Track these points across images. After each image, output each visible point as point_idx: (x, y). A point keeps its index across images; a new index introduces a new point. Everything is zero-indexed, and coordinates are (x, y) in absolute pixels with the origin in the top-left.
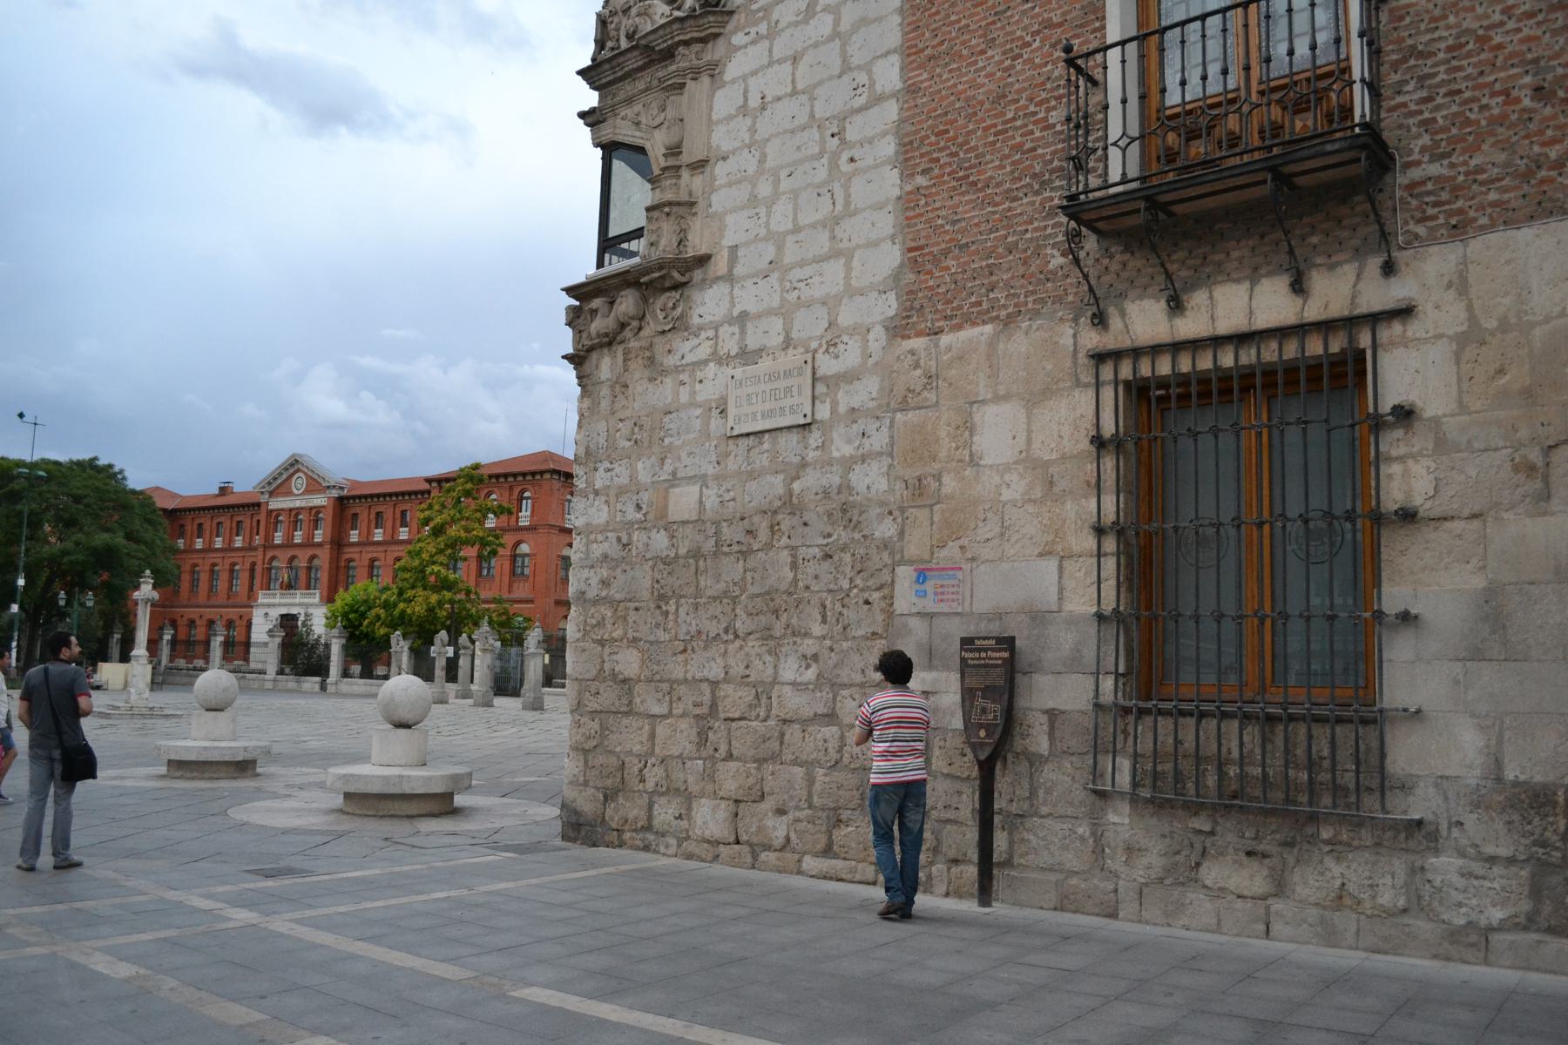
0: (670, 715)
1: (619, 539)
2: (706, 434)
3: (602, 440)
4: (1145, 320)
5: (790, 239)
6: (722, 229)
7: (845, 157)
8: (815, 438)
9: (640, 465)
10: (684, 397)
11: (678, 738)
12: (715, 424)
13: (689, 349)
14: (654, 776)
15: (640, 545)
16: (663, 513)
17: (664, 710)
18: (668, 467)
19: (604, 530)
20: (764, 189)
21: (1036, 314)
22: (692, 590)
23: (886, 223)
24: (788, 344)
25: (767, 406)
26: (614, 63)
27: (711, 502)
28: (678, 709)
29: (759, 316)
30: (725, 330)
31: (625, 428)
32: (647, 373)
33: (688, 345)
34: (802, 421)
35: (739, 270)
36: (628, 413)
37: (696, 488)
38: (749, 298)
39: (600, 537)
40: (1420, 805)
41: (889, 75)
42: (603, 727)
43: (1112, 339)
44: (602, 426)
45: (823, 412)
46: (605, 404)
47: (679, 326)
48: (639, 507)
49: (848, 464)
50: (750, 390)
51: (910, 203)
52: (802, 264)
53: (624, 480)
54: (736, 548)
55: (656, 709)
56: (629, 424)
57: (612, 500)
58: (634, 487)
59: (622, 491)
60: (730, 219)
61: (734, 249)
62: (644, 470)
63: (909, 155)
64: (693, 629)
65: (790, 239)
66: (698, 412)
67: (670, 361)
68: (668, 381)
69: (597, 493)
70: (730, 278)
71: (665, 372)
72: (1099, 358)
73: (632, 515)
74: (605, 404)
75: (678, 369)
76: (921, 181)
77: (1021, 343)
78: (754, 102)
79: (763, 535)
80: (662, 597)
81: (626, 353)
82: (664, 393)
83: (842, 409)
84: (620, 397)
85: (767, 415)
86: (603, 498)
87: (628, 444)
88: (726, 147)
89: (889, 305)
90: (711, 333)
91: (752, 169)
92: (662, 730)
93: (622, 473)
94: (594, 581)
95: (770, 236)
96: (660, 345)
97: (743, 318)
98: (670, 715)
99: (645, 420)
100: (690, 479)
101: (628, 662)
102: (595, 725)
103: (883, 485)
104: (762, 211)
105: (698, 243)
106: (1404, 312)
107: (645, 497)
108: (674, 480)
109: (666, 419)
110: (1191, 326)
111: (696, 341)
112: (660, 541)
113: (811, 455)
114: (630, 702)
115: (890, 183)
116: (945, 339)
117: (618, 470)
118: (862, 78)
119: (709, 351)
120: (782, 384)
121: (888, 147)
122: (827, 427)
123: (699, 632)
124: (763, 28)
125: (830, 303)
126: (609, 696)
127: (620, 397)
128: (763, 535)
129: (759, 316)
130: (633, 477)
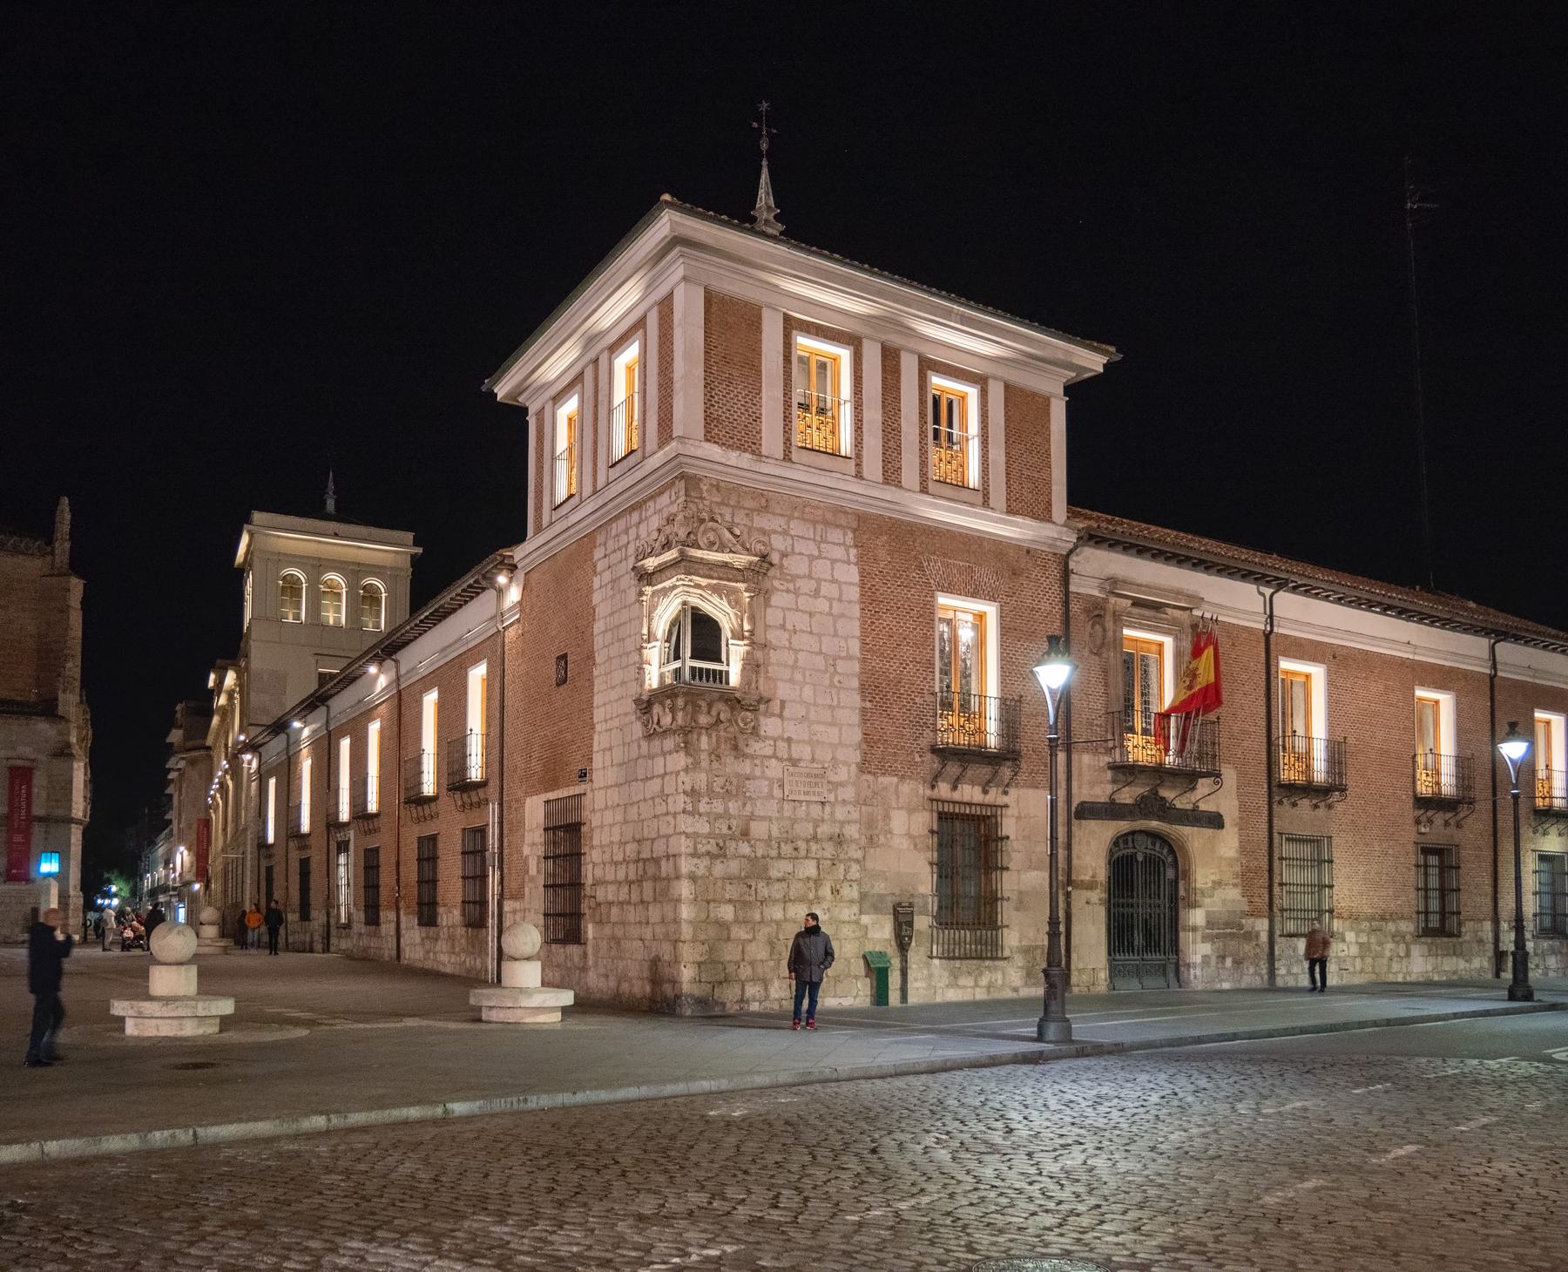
2: (771, 796)
4: (944, 790)
5: (812, 709)
6: (775, 687)
7: (837, 678)
8: (828, 808)
10: (758, 772)
12: (777, 792)
13: (755, 747)
14: (745, 972)
17: (750, 937)
18: (749, 807)
19: (708, 836)
20: (798, 677)
21: (910, 778)
23: (855, 718)
24: (813, 760)
27: (775, 833)
29: (799, 742)
30: (780, 744)
31: (721, 781)
33: (760, 744)
35: (786, 713)
37: (766, 824)
38: (792, 730)
40: (1007, 953)
41: (855, 647)
43: (935, 794)
44: (703, 776)
45: (832, 798)
46: (705, 764)
47: (755, 732)
49: (842, 823)
51: (864, 710)
52: (819, 723)
56: (722, 780)
58: (726, 815)
59: (718, 817)
60: (779, 684)
61: (783, 703)
62: (733, 806)
63: (863, 689)
65: (812, 709)
67: (748, 751)
70: (781, 716)
71: (745, 756)
72: (932, 800)
73: (725, 830)
74: (705, 764)
75: (752, 757)
76: (869, 705)
77: (906, 788)
79: (803, 853)
81: (718, 737)
82: (746, 767)
89: (856, 757)
91: (791, 663)
92: (748, 948)
93: (718, 806)
95: (803, 702)
96: (741, 738)
97: (789, 740)
99: (735, 781)
100: (763, 818)
101: (727, 913)
103: (856, 836)
105: (764, 688)
106: (1007, 806)
107: (734, 823)
108: (752, 817)
110: (956, 796)
113: (826, 817)
115: (856, 699)
116: (881, 779)
118: (843, 644)
120: (813, 780)
121: (855, 683)
122: (833, 805)
124: (791, 586)
125: (834, 747)
128: (803, 853)
129: (799, 742)
130: (726, 810)
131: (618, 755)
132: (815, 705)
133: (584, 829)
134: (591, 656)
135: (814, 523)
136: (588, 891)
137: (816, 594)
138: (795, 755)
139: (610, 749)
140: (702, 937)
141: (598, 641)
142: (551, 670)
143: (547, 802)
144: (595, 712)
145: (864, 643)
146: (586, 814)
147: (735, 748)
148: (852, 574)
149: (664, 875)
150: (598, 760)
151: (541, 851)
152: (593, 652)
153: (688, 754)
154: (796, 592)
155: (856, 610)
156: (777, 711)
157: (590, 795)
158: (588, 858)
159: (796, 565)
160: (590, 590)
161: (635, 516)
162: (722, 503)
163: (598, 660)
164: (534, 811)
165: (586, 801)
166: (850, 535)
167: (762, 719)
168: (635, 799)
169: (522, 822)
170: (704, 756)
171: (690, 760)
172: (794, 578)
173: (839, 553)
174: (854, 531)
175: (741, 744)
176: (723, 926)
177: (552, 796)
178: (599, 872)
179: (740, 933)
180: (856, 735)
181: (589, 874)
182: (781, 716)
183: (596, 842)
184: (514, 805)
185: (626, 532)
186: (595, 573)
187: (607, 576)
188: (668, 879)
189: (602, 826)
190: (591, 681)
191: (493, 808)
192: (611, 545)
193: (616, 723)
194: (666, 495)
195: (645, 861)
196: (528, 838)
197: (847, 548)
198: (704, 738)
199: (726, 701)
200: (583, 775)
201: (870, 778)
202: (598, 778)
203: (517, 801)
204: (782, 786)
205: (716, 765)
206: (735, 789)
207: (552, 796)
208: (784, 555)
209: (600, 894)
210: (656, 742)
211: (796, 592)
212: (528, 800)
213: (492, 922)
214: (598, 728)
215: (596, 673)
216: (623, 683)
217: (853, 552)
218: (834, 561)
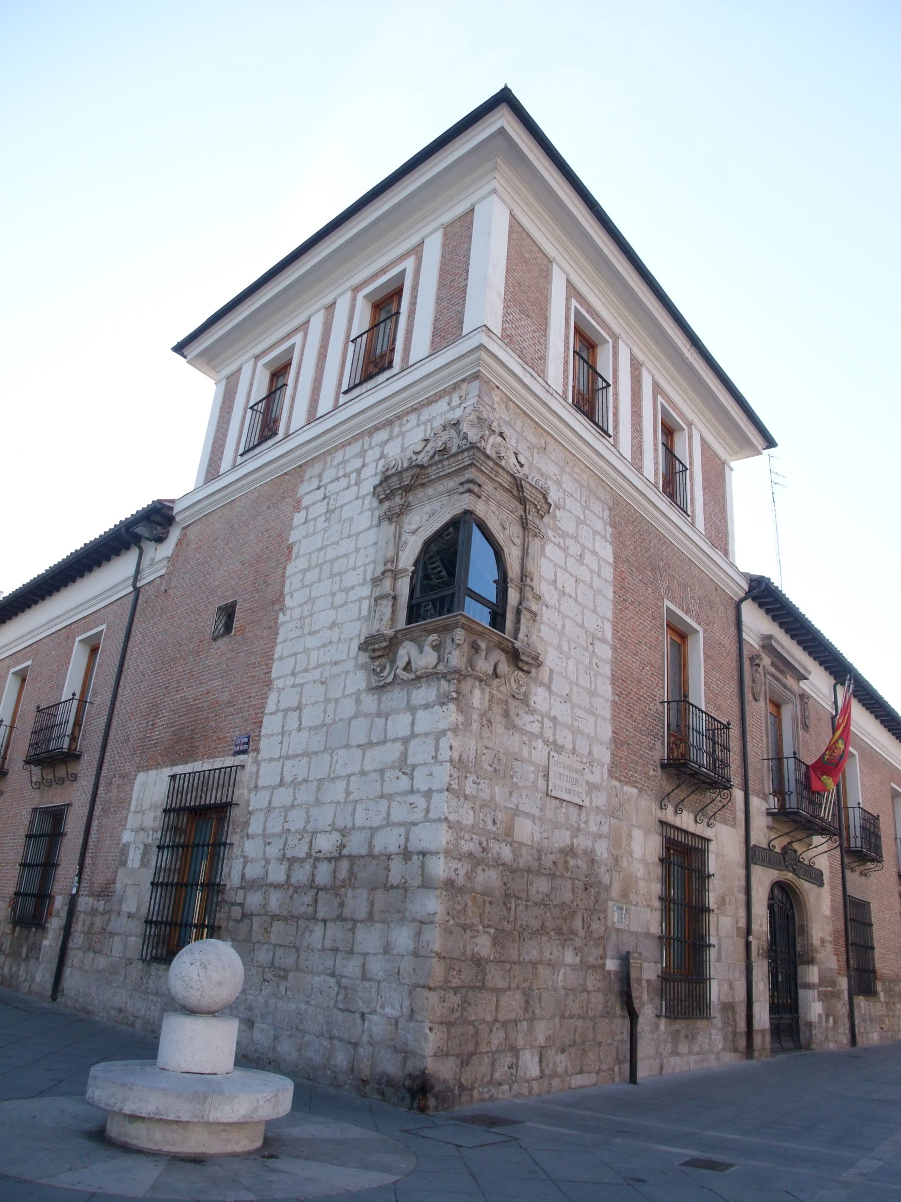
0: (509, 988)
1: (480, 843)
3: (472, 757)
9: (497, 789)
11: (512, 1004)
15: (494, 852)
16: (509, 832)
17: (505, 985)
19: (473, 829)
22: (524, 896)
25: (568, 786)
26: (496, 468)
28: (513, 985)
32: (504, 721)
33: (528, 718)
34: (581, 804)
36: (490, 744)
39: (467, 836)
42: (465, 1001)
45: (587, 803)
46: (475, 727)
47: (524, 700)
48: (494, 822)
50: (561, 771)
53: (486, 795)
54: (548, 872)
55: (502, 984)
57: (477, 808)
59: (484, 805)
64: (524, 923)
66: (533, 769)
67: (519, 722)
68: (517, 735)
69: (466, 797)
74: (475, 727)
75: (523, 732)
78: (560, 586)
80: (507, 895)
81: (492, 696)
82: (514, 742)
83: (594, 805)
84: (485, 728)
85: (568, 791)
86: (471, 805)
87: (490, 769)
88: (547, 598)
90: (540, 719)
94: (462, 872)
97: (554, 720)
98: (509, 988)
101: (483, 945)
102: (456, 999)
104: (564, 660)
107: (500, 816)
109: (515, 763)
111: (531, 718)
112: (506, 853)
114: (484, 980)
117: (482, 786)
119: (546, 736)
123: (527, 926)
124: (561, 541)
126: (468, 975)
127: (485, 728)
131: (311, 716)
132: (578, 685)
133: (235, 812)
134: (278, 602)
135: (582, 486)
136: (229, 896)
137: (581, 560)
138: (560, 741)
139: (299, 708)
140: (455, 982)
141: (292, 583)
142: (209, 621)
143: (173, 777)
144: (276, 666)
145: (615, 631)
146: (241, 793)
147: (506, 714)
148: (607, 552)
149: (395, 877)
150: (271, 724)
151: (153, 838)
152: (282, 595)
153: (461, 710)
154: (565, 549)
155: (609, 592)
156: (546, 681)
157: (250, 768)
158: (236, 851)
159: (566, 522)
160: (289, 527)
161: (382, 435)
162: (508, 423)
163: (288, 602)
164: (151, 790)
165: (244, 777)
166: (607, 513)
167: (532, 685)
168: (341, 771)
169: (124, 803)
170: (475, 716)
171: (461, 718)
172: (564, 535)
173: (599, 525)
174: (610, 510)
175: (512, 712)
176: (478, 962)
177: (179, 769)
178: (253, 871)
179: (495, 977)
180: (606, 732)
181: (233, 872)
182: (549, 688)
183: (255, 827)
184: (117, 781)
185: (362, 453)
186: (297, 507)
187: (321, 508)
188: (404, 888)
189: (269, 809)
190: (274, 629)
191: (85, 782)
192: (329, 474)
193: (316, 675)
194: (446, 399)
195: (352, 858)
196: (133, 821)
197: (605, 524)
198: (477, 693)
199: (503, 650)
200: (246, 746)
201: (616, 783)
202: (268, 746)
203: (123, 776)
204: (546, 777)
205: (486, 733)
206: (502, 769)
207: (179, 769)
208: (558, 507)
209: (254, 900)
210: (396, 698)
211: (565, 549)
212: (141, 777)
213: (55, 924)
214: (278, 684)
215: (282, 618)
216: (334, 624)
217: (609, 530)
218: (596, 533)
